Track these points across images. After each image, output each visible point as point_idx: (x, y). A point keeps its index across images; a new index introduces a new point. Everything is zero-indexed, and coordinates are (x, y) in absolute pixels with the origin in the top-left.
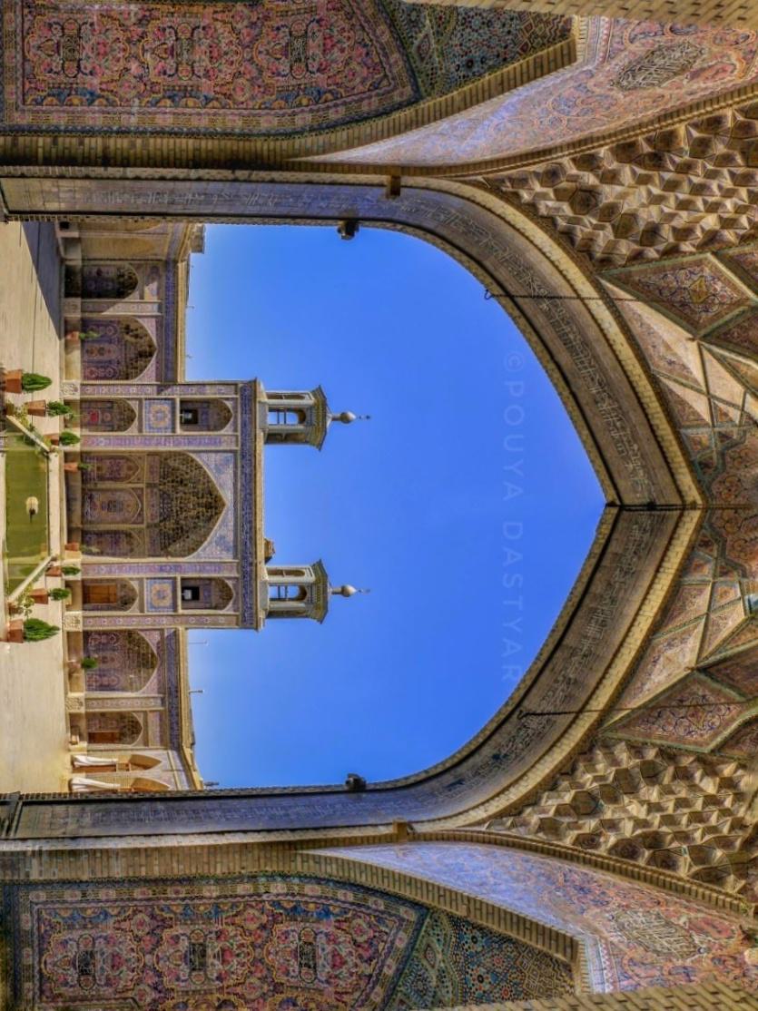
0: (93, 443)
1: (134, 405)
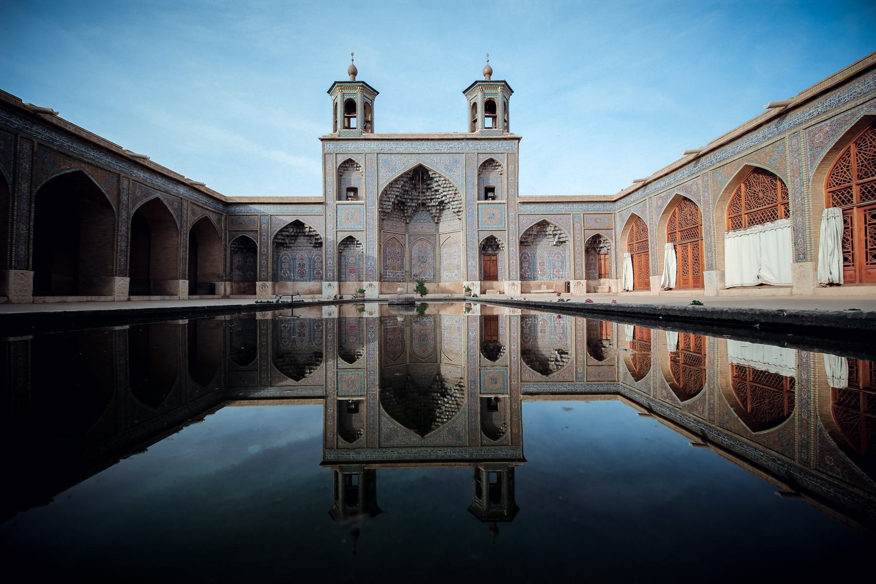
1: (342, 236)
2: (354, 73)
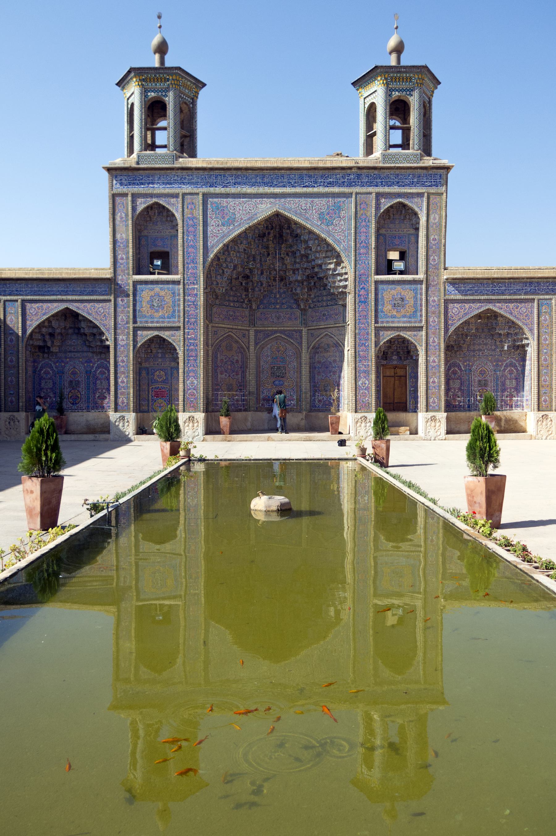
0: (193, 395)
1: (144, 336)
2: (162, 49)
